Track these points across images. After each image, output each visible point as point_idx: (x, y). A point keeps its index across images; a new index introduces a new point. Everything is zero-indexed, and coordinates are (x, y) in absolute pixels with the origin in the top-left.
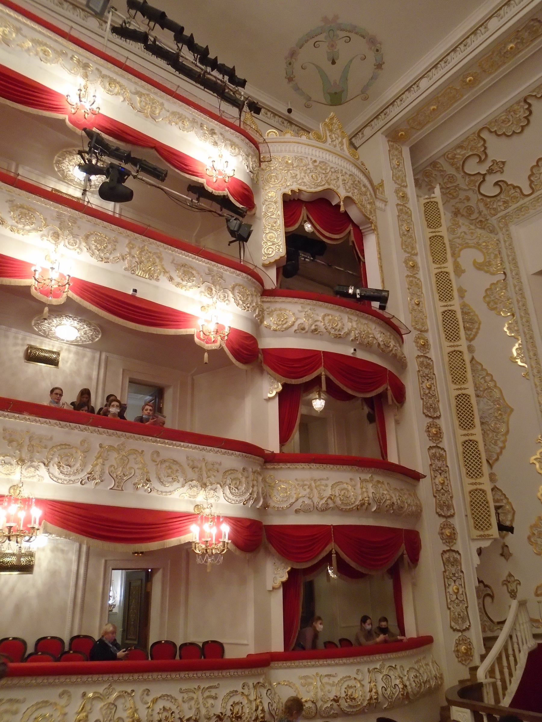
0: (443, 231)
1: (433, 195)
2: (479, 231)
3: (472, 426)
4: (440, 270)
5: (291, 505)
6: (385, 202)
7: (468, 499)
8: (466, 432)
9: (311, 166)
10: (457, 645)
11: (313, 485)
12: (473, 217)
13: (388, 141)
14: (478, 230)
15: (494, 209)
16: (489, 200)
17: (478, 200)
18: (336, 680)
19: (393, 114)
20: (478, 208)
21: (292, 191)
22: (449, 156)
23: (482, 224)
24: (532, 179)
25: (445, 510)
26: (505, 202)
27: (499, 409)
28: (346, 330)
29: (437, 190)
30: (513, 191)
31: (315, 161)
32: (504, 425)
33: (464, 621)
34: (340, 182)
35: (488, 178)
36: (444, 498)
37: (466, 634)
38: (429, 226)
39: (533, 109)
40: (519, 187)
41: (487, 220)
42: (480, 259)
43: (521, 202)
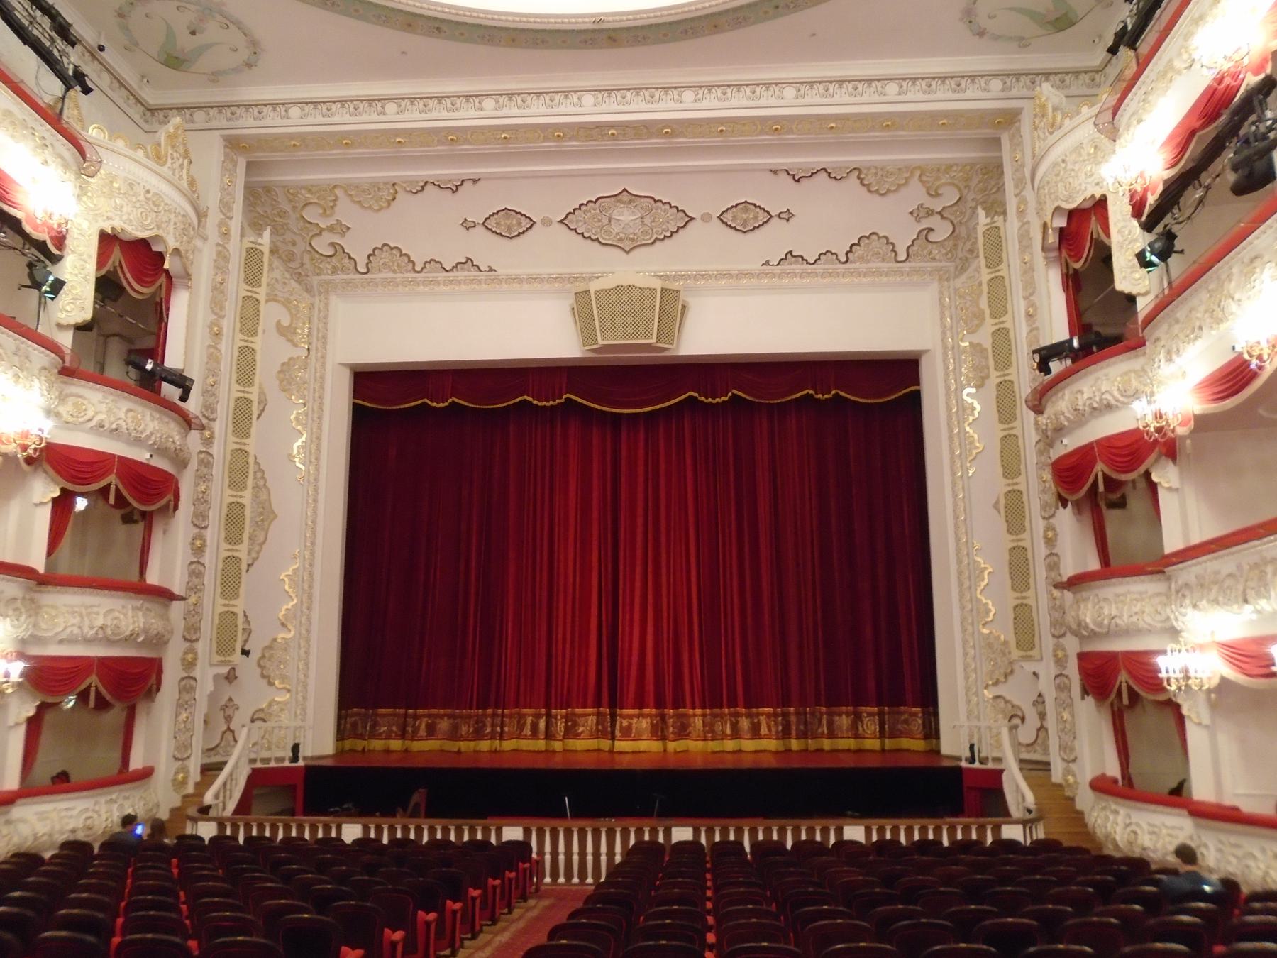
0: (262, 293)
1: (260, 241)
2: (294, 284)
3: (240, 541)
5: (57, 634)
6: (205, 239)
7: (216, 621)
8: (230, 547)
9: (142, 198)
10: (177, 773)
11: (84, 611)
13: (225, 146)
14: (293, 283)
17: (306, 251)
18: (75, 812)
19: (240, 123)
20: (302, 258)
22: (292, 192)
23: (299, 277)
25: (191, 634)
26: (334, 267)
27: (261, 514)
28: (148, 433)
29: (267, 233)
30: (347, 260)
31: (148, 192)
32: (263, 533)
33: (186, 750)
34: (171, 228)
35: (325, 234)
36: (193, 620)
37: (186, 762)
38: (246, 281)
39: (398, 196)
42: (286, 323)
43: (351, 276)
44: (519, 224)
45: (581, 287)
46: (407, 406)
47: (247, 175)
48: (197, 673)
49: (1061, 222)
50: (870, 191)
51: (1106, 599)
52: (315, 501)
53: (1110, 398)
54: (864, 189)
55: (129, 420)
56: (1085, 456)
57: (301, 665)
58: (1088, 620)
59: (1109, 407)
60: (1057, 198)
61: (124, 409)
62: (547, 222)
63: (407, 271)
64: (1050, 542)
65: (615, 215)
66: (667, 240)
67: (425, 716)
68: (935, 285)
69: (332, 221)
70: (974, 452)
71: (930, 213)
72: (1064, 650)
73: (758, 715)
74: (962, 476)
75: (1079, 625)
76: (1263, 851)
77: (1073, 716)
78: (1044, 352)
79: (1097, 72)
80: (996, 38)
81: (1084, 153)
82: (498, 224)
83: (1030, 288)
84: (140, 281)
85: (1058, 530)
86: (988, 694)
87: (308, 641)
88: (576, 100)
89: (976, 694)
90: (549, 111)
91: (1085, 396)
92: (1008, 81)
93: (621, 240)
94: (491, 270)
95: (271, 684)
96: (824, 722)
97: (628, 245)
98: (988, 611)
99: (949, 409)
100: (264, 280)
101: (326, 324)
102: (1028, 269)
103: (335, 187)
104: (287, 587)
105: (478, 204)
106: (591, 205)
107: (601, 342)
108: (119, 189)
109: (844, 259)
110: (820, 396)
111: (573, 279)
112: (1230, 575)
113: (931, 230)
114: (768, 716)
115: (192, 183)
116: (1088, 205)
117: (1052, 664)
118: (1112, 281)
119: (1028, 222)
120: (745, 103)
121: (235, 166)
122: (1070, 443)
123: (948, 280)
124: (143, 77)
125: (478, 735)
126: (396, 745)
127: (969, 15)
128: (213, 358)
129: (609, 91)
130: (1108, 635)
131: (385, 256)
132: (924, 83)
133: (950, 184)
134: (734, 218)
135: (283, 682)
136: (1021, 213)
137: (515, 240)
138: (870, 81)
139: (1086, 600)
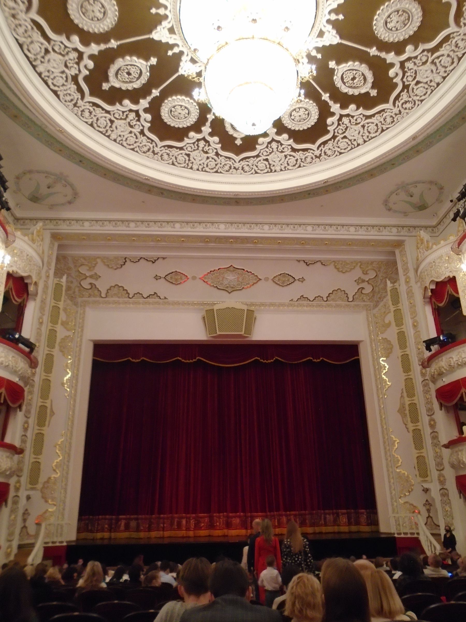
1: (61, 280)
2: (69, 302)
4: (52, 328)
7: (30, 467)
9: (25, 258)
10: (8, 548)
12: (69, 292)
15: (83, 295)
16: (82, 289)
21: (13, 271)
23: (72, 298)
24: (109, 291)
26: (89, 294)
28: (20, 368)
29: (65, 277)
30: (96, 292)
31: (28, 255)
35: (88, 279)
39: (126, 263)
40: (100, 291)
41: (75, 298)
43: (98, 299)
45: (208, 308)
46: (120, 361)
47: (58, 251)
48: (20, 494)
49: (433, 287)
50: (339, 271)
52: (74, 406)
54: (336, 270)
55: (13, 362)
56: (456, 386)
57: (62, 491)
60: (432, 277)
61: (11, 356)
62: (194, 278)
63: (125, 297)
64: (432, 426)
65: (226, 276)
66: (248, 289)
67: (124, 519)
68: (364, 313)
69: (92, 273)
70: (387, 386)
71: (363, 281)
72: (444, 476)
73: (290, 515)
74: (382, 398)
75: (459, 462)
77: (451, 508)
78: (428, 342)
79: (434, 227)
80: (395, 211)
81: (443, 259)
82: (171, 278)
83: (414, 314)
84: (19, 297)
85: (436, 421)
86: (401, 501)
87: (67, 479)
88: (217, 226)
89: (396, 501)
90: (205, 230)
91: (455, 360)
92: (399, 229)
93: (227, 287)
94: (165, 298)
95: (46, 501)
96: (323, 518)
97: (230, 290)
98: (399, 461)
99: (375, 367)
100: (63, 299)
101: (83, 320)
102: (412, 306)
103: (98, 258)
104: (57, 451)
105: (162, 269)
107: (218, 333)
108: (17, 253)
109: (325, 300)
110: (315, 360)
111: (203, 304)
114: (295, 515)
115: (43, 252)
116: (446, 280)
117: (438, 483)
119: (411, 286)
120: (291, 231)
121: (53, 245)
123: (370, 310)
124: (17, 205)
125: (149, 530)
126: (106, 535)
127: (386, 202)
128: (39, 334)
131: (115, 290)
132: (365, 228)
133: (372, 269)
134: (279, 280)
135: (53, 500)
136: (407, 282)
137: (178, 286)
138: (343, 226)
139: (461, 450)
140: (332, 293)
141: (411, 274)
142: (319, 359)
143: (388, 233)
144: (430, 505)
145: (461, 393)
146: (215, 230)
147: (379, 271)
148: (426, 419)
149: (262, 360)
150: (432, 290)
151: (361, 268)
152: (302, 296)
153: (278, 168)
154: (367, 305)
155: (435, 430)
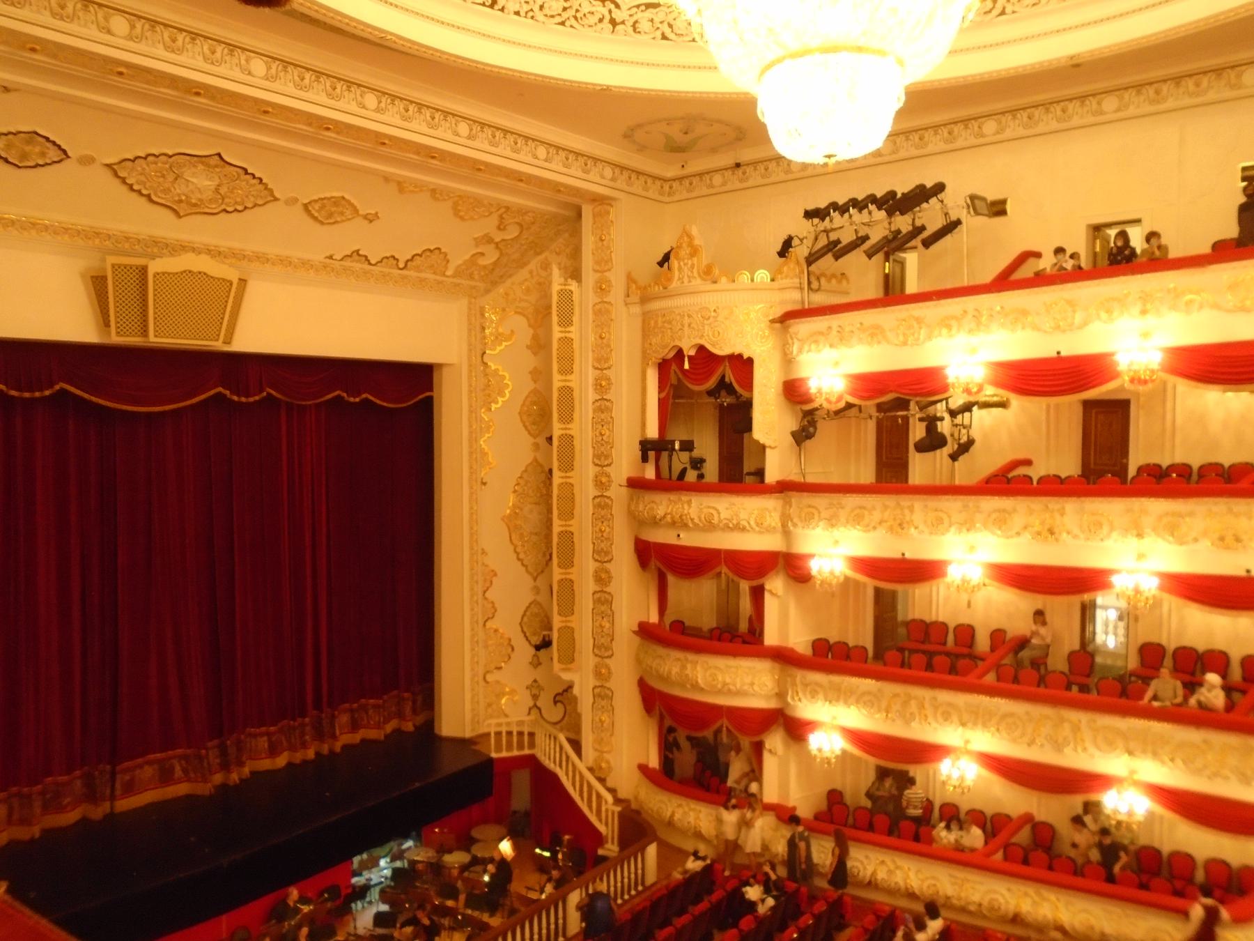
44: (43, 154)
49: (692, 353)
51: (720, 669)
53: (745, 523)
58: (700, 681)
59: (743, 529)
62: (87, 161)
68: (464, 302)
76: (867, 857)
88: (243, 62)
93: (180, 201)
106: (163, 158)
109: (401, 266)
112: (869, 693)
113: (482, 254)
117: (591, 676)
118: (748, 427)
122: (689, 539)
129: (286, 64)
130: (719, 692)
136: (602, 288)
138: (527, 138)
140: (420, 255)
141: (617, 279)
142: (359, 395)
143: (598, 179)
144: (540, 688)
145: (718, 570)
146: (237, 74)
147: (528, 228)
148: (591, 566)
149: (235, 398)
150: (690, 358)
151: (501, 217)
152: (357, 251)
153: (512, 7)
154: (474, 287)
155: (608, 589)
